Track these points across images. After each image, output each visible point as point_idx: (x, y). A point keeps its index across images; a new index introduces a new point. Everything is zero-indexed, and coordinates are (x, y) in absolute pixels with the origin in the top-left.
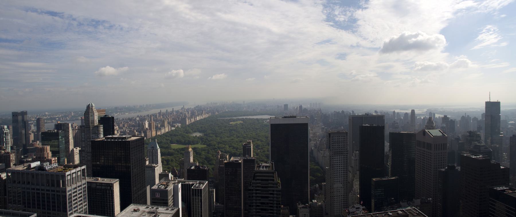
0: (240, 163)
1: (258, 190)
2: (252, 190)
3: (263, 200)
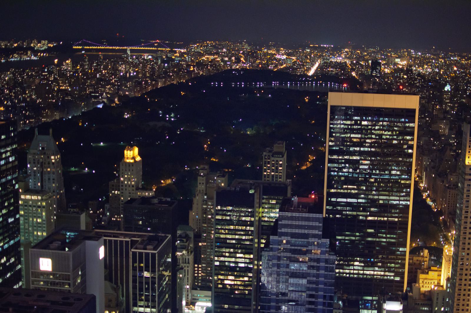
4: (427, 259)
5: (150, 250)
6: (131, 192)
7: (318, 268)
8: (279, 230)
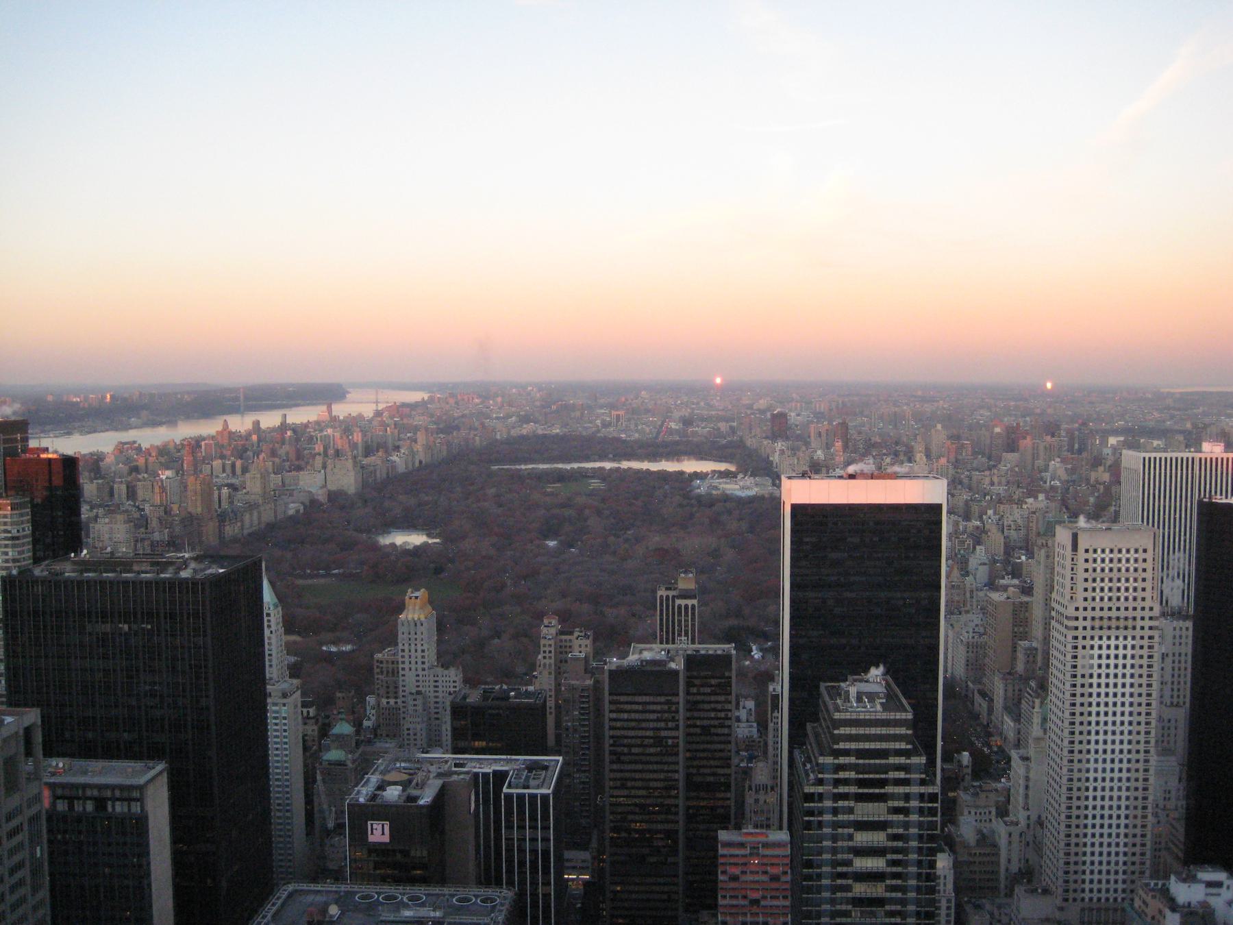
0: (676, 673)
1: (845, 797)
2: (821, 795)
3: (862, 838)
4: (969, 771)
5: (538, 787)
6: (421, 673)
7: (905, 811)
8: (836, 747)
